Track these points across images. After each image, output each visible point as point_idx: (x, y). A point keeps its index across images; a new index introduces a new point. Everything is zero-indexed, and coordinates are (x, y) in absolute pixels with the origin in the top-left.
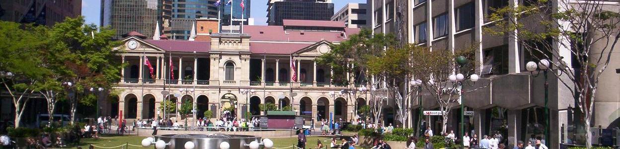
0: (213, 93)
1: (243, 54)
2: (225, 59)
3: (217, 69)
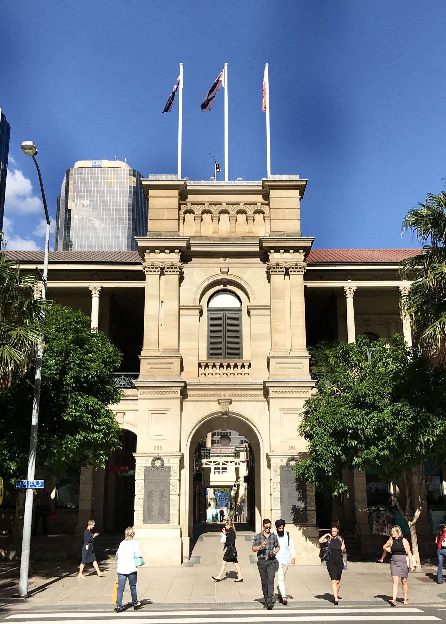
0: (155, 412)
1: (277, 249)
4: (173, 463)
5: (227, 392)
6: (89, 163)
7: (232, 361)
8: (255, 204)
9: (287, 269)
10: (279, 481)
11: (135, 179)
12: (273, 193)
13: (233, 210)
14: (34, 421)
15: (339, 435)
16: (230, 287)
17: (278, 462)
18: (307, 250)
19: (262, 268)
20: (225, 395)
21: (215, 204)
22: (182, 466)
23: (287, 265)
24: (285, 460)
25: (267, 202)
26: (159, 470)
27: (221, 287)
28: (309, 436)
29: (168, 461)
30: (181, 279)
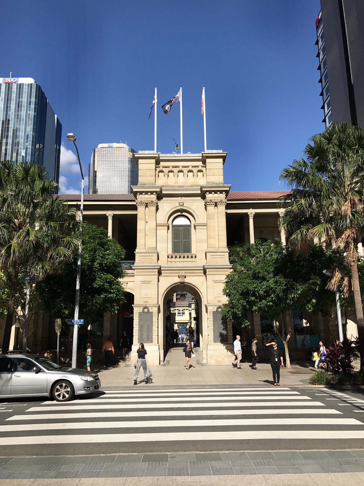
0: (144, 282)
1: (210, 192)
2: (167, 206)
3: (152, 235)
4: (155, 310)
5: (183, 272)
6: (106, 145)
7: (186, 254)
8: (198, 167)
9: (216, 203)
10: (212, 319)
11: (132, 154)
12: (208, 160)
13: (185, 170)
14: (78, 287)
15: (245, 294)
16: (184, 214)
17: (211, 309)
18: (227, 192)
19: (202, 203)
20: (182, 273)
21: (176, 167)
22: (159, 312)
23: (216, 201)
24: (216, 308)
25: (205, 165)
26: (146, 314)
27: (179, 213)
28: (228, 295)
29: (152, 309)
30: (157, 209)
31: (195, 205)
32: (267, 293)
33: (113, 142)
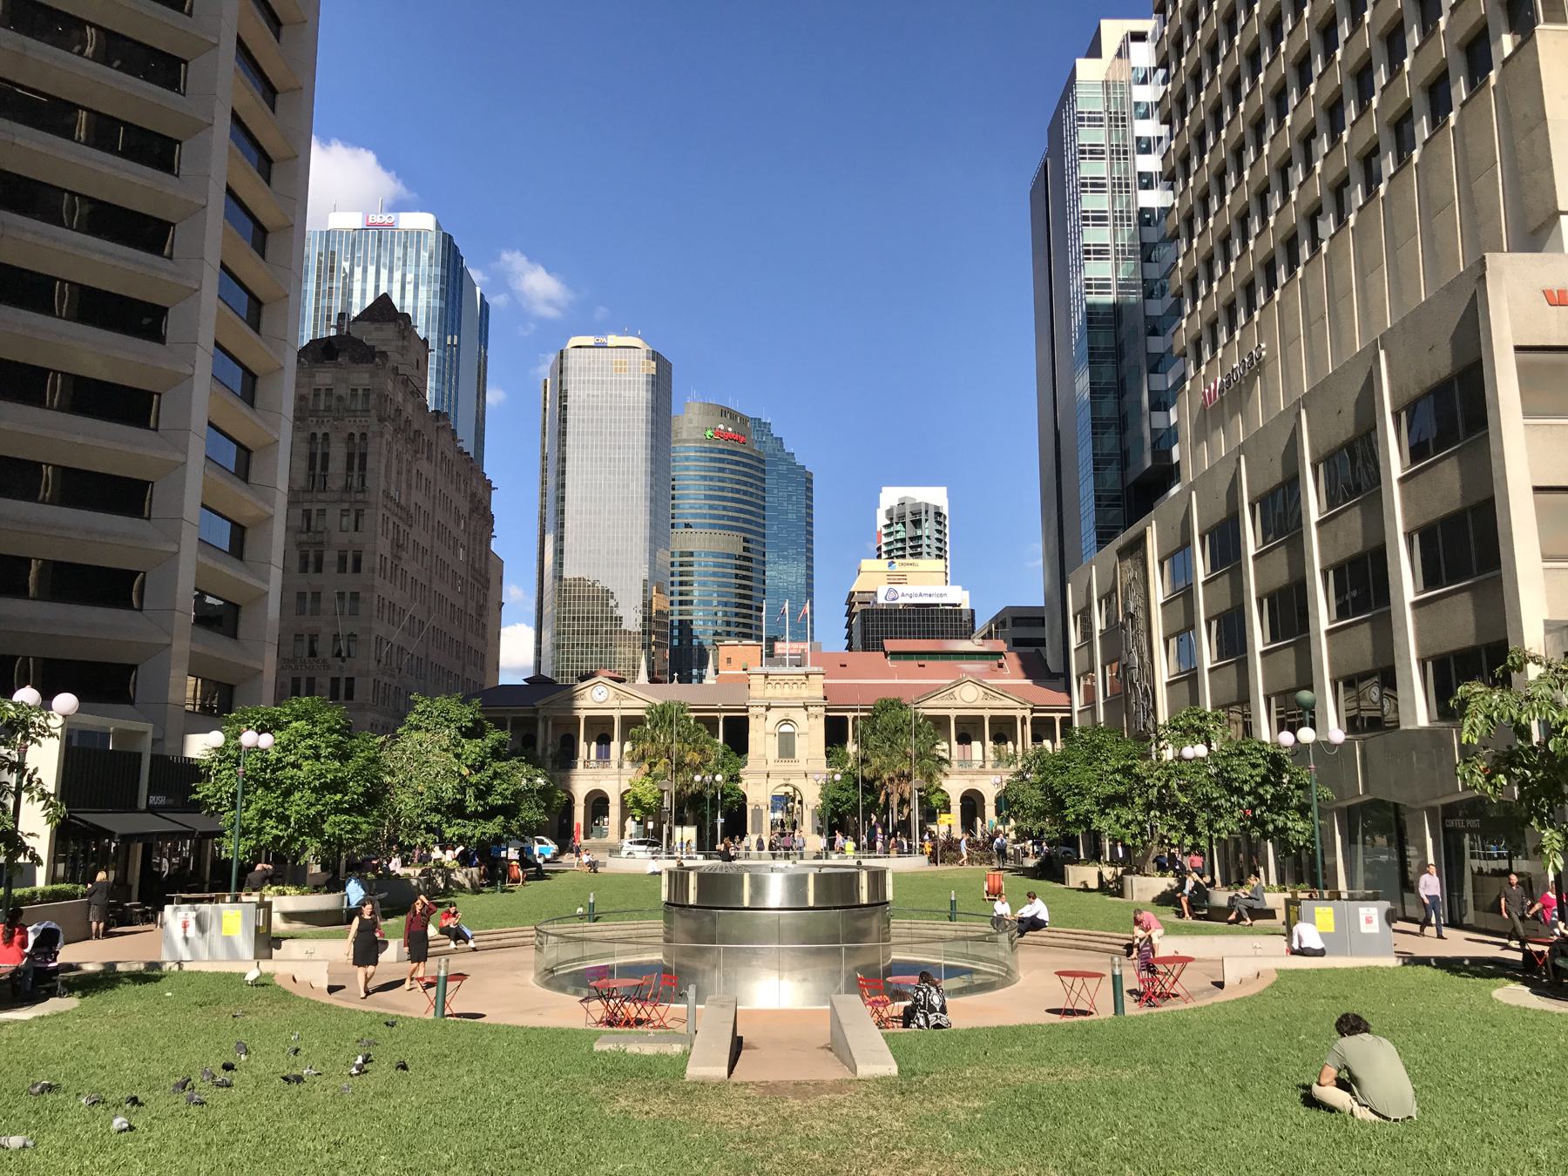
2: (775, 716)
3: (761, 739)
6: (589, 340)
11: (654, 364)
15: (834, 800)
17: (811, 807)
26: (758, 812)
31: (799, 715)
32: (848, 799)
33: (603, 333)
